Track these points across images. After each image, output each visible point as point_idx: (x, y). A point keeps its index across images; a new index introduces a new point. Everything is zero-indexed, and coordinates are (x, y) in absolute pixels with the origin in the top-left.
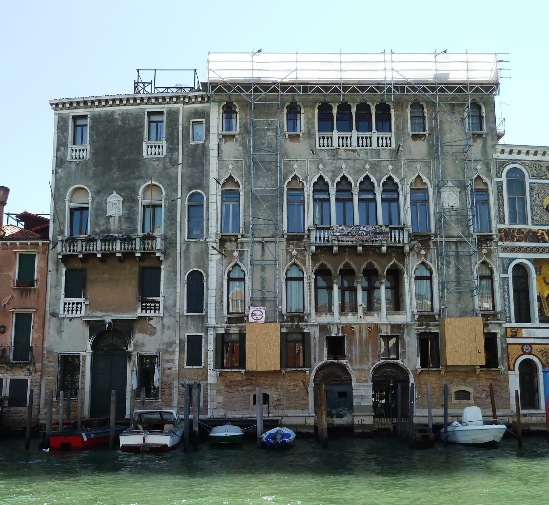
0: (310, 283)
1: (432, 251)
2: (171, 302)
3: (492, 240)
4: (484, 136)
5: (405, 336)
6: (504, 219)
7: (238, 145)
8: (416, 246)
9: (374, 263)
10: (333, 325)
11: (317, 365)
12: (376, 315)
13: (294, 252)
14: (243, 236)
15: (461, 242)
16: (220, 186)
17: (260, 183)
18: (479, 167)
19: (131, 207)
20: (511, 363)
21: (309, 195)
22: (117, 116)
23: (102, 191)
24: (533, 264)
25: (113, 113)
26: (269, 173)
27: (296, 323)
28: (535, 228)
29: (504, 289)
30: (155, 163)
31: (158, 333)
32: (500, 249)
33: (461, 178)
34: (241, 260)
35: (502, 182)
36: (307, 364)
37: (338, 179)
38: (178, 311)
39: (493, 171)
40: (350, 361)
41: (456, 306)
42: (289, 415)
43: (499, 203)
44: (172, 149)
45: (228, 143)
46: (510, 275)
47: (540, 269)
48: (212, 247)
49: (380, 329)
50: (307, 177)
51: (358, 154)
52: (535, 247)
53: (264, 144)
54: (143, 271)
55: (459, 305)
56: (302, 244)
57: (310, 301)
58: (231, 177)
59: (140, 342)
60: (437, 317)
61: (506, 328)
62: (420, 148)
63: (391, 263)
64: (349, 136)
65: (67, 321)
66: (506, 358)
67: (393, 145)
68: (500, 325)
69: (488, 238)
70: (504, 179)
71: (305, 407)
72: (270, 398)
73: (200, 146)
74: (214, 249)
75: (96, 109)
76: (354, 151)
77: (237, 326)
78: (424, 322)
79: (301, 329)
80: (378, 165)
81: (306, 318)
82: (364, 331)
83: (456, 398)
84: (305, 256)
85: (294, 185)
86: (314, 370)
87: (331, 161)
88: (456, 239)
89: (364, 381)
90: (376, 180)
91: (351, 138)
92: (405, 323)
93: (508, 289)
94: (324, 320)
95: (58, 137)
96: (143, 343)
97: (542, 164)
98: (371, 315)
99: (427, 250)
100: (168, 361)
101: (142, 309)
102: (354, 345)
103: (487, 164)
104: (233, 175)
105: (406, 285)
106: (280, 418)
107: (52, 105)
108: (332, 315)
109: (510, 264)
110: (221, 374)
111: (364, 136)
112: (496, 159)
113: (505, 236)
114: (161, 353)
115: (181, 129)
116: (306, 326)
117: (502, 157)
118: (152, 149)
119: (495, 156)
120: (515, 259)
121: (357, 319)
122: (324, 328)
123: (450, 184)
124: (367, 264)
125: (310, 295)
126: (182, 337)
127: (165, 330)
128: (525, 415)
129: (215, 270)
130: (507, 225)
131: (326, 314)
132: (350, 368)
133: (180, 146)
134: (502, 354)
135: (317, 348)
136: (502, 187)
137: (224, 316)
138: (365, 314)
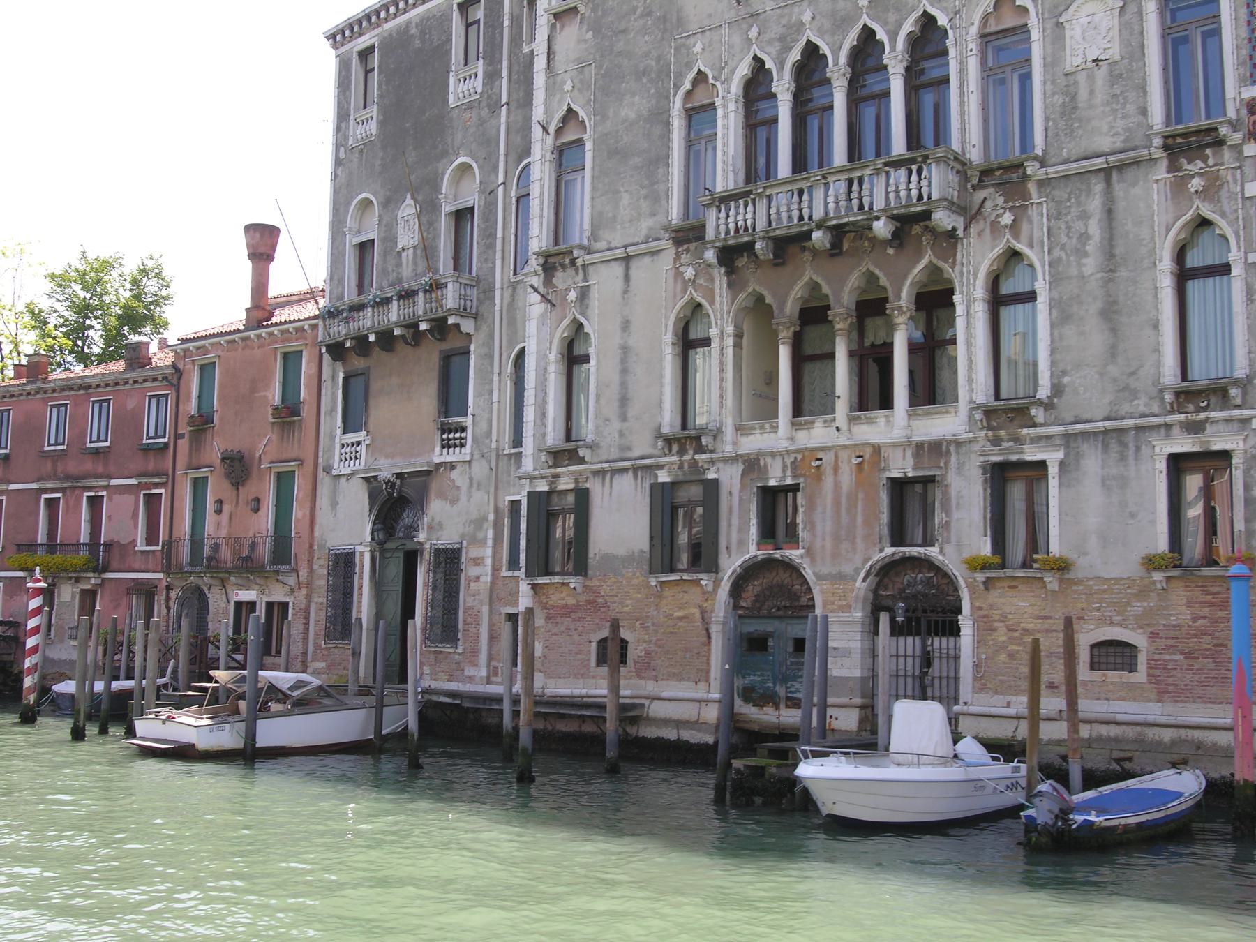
1: (1033, 213)
2: (483, 426)
3: (1220, 143)
7: (585, 28)
8: (988, 204)
9: (877, 271)
10: (773, 455)
11: (731, 564)
12: (883, 420)
13: (689, 273)
14: (589, 251)
15: (1121, 167)
22: (413, 31)
25: (409, 23)
30: (466, 115)
31: (463, 498)
38: (494, 445)
40: (809, 552)
41: (1101, 374)
42: (664, 695)
44: (492, 77)
45: (567, 30)
48: (532, 286)
53: (635, 9)
55: (1113, 370)
57: (721, 397)
58: (570, 110)
59: (437, 520)
63: (920, 266)
65: (343, 480)
69: (1208, 139)
71: (703, 676)
72: (630, 647)
74: (536, 290)
75: (387, 26)
77: (570, 473)
83: (1093, 666)
84: (712, 280)
85: (700, 99)
86: (726, 578)
87: (779, 11)
88: (1102, 159)
90: (887, 32)
92: (949, 437)
94: (753, 443)
95: (339, 103)
98: (870, 421)
99: (1020, 213)
100: (478, 561)
101: (443, 447)
102: (819, 510)
104: (573, 106)
106: (647, 702)
107: (328, 38)
108: (775, 428)
114: (465, 543)
115: (506, 23)
116: (712, 462)
118: (462, 88)
121: (837, 431)
122: (752, 464)
127: (474, 490)
131: (762, 427)
132: (809, 574)
133: (505, 64)
135: (735, 521)
138: (852, 420)
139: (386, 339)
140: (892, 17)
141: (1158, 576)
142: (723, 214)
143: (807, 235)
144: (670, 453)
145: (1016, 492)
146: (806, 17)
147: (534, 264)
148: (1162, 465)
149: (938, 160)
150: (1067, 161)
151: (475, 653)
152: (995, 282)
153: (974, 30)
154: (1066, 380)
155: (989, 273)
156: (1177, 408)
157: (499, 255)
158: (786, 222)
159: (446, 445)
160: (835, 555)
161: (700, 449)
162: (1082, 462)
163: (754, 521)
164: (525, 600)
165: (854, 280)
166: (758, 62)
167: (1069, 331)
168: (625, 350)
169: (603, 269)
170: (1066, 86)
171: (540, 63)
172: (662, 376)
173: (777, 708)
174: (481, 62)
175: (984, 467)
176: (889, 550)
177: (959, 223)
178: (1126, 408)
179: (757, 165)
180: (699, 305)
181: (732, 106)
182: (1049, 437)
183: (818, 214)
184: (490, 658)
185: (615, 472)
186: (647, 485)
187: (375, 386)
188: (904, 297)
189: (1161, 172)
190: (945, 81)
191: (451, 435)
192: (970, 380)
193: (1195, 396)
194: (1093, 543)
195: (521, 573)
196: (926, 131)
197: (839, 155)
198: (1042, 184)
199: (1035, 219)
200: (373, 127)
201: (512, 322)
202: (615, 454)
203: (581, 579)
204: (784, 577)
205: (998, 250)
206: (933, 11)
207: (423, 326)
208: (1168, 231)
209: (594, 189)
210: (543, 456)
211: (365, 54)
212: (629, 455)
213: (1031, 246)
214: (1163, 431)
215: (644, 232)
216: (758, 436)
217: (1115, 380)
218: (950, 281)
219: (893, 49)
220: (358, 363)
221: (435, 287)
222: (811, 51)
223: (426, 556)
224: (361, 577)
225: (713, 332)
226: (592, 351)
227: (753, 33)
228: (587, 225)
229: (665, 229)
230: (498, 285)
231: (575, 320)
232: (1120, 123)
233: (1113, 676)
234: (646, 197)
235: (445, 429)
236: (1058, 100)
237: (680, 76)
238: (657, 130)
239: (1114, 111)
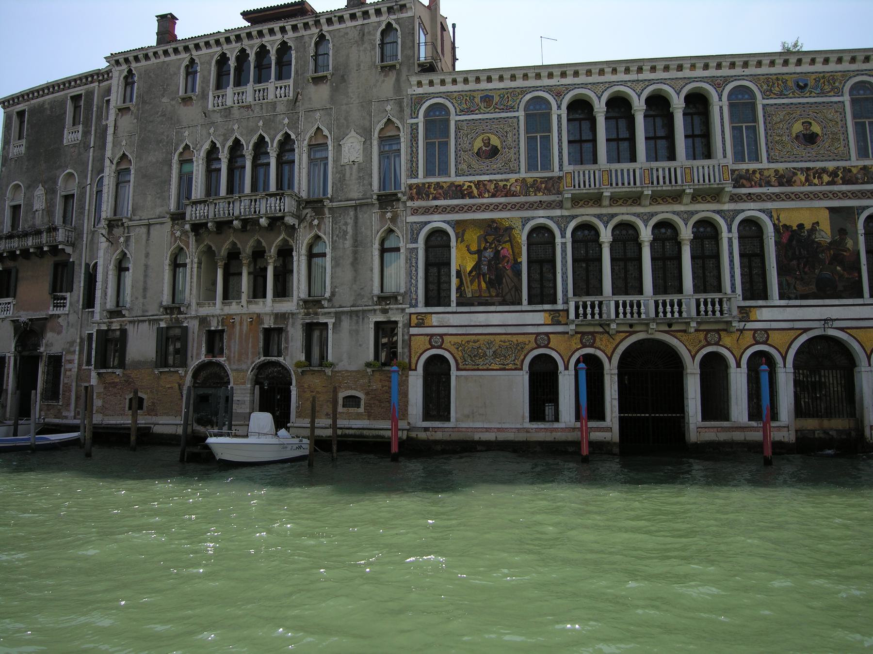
1: (326, 220)
3: (398, 200)
4: (398, 67)
5: (289, 328)
8: (309, 215)
10: (213, 316)
11: (193, 364)
13: (178, 234)
14: (131, 220)
15: (361, 205)
18: (389, 108)
19: (52, 199)
20: (414, 361)
23: (31, 187)
24: (453, 228)
25: (44, 102)
28: (460, 180)
30: (72, 150)
31: (64, 331)
32: (409, 211)
33: (367, 124)
35: (417, 124)
36: (184, 364)
39: (407, 111)
40: (228, 359)
42: (161, 422)
44: (86, 133)
45: (124, 117)
46: (421, 244)
47: (463, 235)
49: (262, 320)
52: (457, 206)
54: (56, 266)
58: (124, 154)
61: (411, 314)
62: (320, 94)
66: (407, 354)
67: (291, 95)
68: (403, 310)
69: (394, 198)
70: (420, 120)
75: (32, 102)
76: (249, 107)
77: (118, 321)
82: (245, 323)
85: (186, 156)
93: (417, 263)
94: (204, 311)
96: (53, 343)
97: (475, 94)
98: (256, 303)
99: (321, 220)
100: (71, 362)
103: (400, 103)
108: (215, 304)
109: (421, 229)
113: (418, 193)
115: (95, 109)
117: (420, 91)
118: (71, 136)
119: (410, 92)
120: (429, 222)
121: (242, 307)
122: (203, 321)
123: (353, 133)
126: (83, 336)
128: (426, 429)
129: (104, 260)
130: (421, 179)
132: (228, 367)
133: (93, 128)
135: (195, 345)
138: (249, 302)
139: (25, 253)
140: (272, 132)
141: (369, 370)
142: (194, 209)
143: (231, 222)
144: (167, 314)
145: (316, 334)
146: (236, 127)
147: (103, 223)
148: (372, 326)
149: (288, 195)
150: (341, 201)
151: (68, 405)
152: (310, 247)
153: (306, 142)
155: (308, 244)
157: (86, 217)
158: (223, 216)
159: (56, 306)
160: (239, 360)
161: (180, 313)
163: (204, 345)
164: (94, 381)
165: (251, 243)
166: (213, 144)
169: (138, 229)
170: (341, 170)
171: (110, 131)
172: (163, 279)
174: (81, 126)
176: (263, 358)
177: (296, 222)
178: (359, 302)
179: (211, 188)
180: (182, 248)
181: (201, 162)
182: (329, 313)
183: (237, 213)
184: (76, 407)
185: (139, 321)
186: (155, 327)
187: (20, 275)
188: (272, 251)
190: (293, 162)
191: (59, 301)
192: (298, 288)
193: (386, 299)
195: (92, 367)
196: (284, 182)
197: (247, 189)
198: (331, 209)
199: (327, 223)
200: (23, 150)
201: (92, 250)
202: (140, 313)
203: (121, 370)
205: (312, 235)
206: (290, 132)
207: (45, 249)
209: (134, 192)
210: (105, 313)
211: (21, 114)
215: (158, 213)
218: (292, 246)
219: (272, 146)
220: (10, 264)
221: (52, 229)
222: (237, 142)
223: (44, 358)
224: (9, 369)
225: (188, 261)
226: (131, 266)
227: (212, 130)
228: (130, 208)
229: (167, 213)
230: (85, 232)
231: (123, 251)
233: (351, 410)
235: (56, 298)
236: (338, 176)
237: (177, 145)
238: (166, 168)
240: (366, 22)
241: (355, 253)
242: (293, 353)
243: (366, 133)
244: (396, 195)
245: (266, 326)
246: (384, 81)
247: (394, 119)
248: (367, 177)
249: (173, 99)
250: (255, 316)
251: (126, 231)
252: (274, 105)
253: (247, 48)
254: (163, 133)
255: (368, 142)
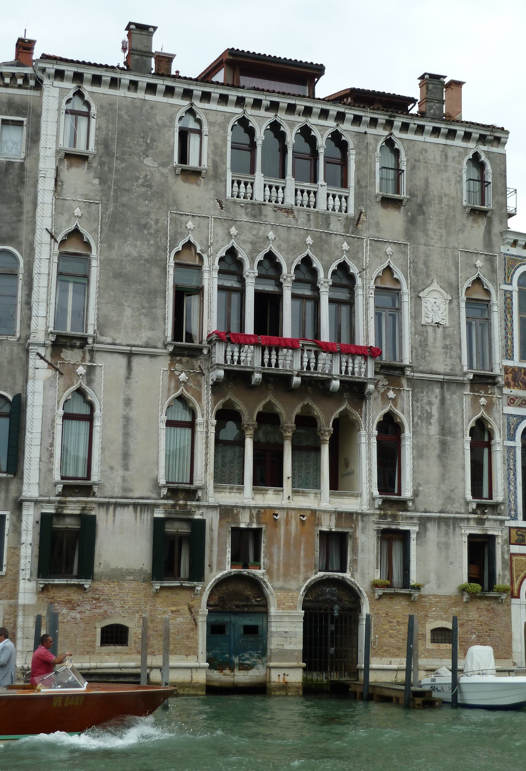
0: (207, 433)
1: (404, 395)
3: (494, 384)
5: (359, 534)
6: (512, 351)
7: (92, 174)
9: (315, 406)
10: (244, 508)
11: (213, 576)
13: (183, 377)
16: (57, 245)
17: (128, 249)
18: (479, 263)
20: (516, 587)
21: (211, 278)
26: (145, 232)
27: (181, 502)
29: (509, 465)
32: (505, 400)
33: (453, 278)
34: (90, 382)
37: (260, 257)
40: (269, 572)
41: (438, 489)
43: (507, 325)
46: (518, 443)
48: (38, 354)
49: (319, 519)
50: (209, 247)
51: (294, 217)
53: (137, 179)
55: (443, 487)
56: (197, 363)
57: (206, 465)
60: (410, 504)
61: (510, 528)
62: (393, 221)
63: (341, 409)
64: (281, 185)
66: (508, 577)
67: (351, 211)
68: (502, 522)
69: (490, 381)
70: (514, 287)
73: (16, 166)
74: (42, 358)
76: (289, 211)
78: (389, 512)
79: (190, 513)
80: (326, 242)
81: (200, 493)
83: (433, 641)
84: (200, 386)
85: (188, 259)
87: (251, 225)
88: (442, 377)
89: (290, 608)
91: (283, 188)
93: (514, 465)
94: (228, 498)
98: (304, 494)
99: (398, 392)
102: (276, 546)
104: (80, 228)
105: (364, 448)
108: (241, 490)
109: (518, 424)
110: (45, 589)
111: (306, 189)
112: (505, 254)
113: (514, 379)
116: (199, 507)
117: (514, 251)
119: (504, 249)
122: (227, 512)
123: (435, 286)
124: (302, 408)
125: (206, 454)
130: (516, 362)
134: (503, 569)
135: (215, 548)
136: (511, 300)
137: (58, 483)
140: (326, 257)
148: (465, 539)
154: (421, 488)
156: (474, 512)
162: (428, 533)
163: (229, 549)
167: (422, 463)
168: (127, 420)
169: (109, 358)
170: (420, 330)
173: (232, 670)
175: (378, 531)
178: (449, 508)
182: (411, 518)
185: (116, 505)
189: (467, 391)
194: (433, 577)
198: (409, 380)
199: (405, 398)
202: (118, 492)
204: (240, 587)
206: (350, 263)
208: (469, 421)
212: (131, 495)
213: (403, 412)
214: (466, 521)
216: (227, 494)
217: (444, 492)
232: (449, 361)
234: (146, 315)
238: (156, 271)
239: (446, 353)
240: (449, 142)
241: (444, 445)
242: (364, 569)
243: (452, 288)
244: (494, 377)
245: (325, 529)
246: (472, 227)
247: (485, 280)
248: (455, 348)
249: (163, 165)
250: (308, 513)
251: (88, 357)
252: (326, 218)
253: (283, 123)
254: (148, 214)
255: (455, 302)
